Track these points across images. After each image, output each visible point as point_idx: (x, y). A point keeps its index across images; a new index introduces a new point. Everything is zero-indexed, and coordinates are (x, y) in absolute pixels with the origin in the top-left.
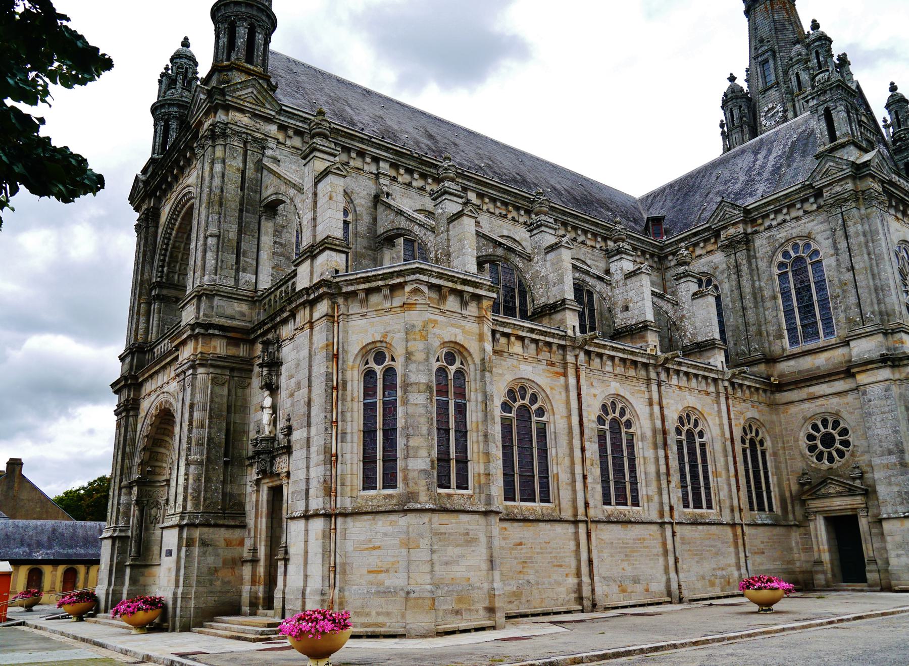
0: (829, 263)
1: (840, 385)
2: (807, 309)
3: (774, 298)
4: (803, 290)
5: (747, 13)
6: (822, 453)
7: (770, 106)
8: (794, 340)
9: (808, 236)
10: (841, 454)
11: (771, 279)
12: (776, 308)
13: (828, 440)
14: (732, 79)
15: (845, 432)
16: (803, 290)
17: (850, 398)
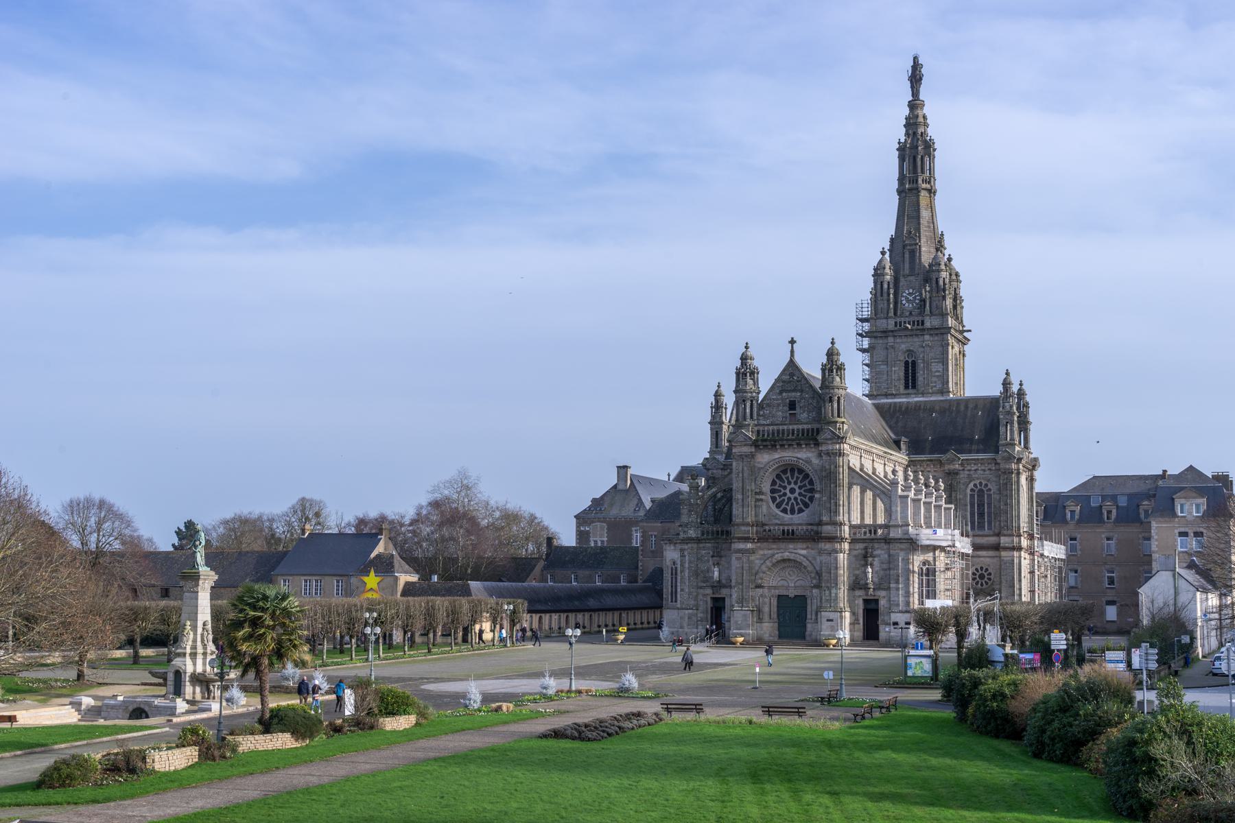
0: (995, 497)
1: (991, 553)
2: (981, 515)
3: (966, 505)
4: (981, 505)
5: (900, 192)
6: (978, 582)
7: (911, 291)
8: (973, 528)
9: (988, 480)
10: (987, 583)
11: (966, 494)
12: (966, 511)
13: (982, 577)
14: (883, 253)
15: (990, 574)
16: (981, 505)
17: (995, 560)
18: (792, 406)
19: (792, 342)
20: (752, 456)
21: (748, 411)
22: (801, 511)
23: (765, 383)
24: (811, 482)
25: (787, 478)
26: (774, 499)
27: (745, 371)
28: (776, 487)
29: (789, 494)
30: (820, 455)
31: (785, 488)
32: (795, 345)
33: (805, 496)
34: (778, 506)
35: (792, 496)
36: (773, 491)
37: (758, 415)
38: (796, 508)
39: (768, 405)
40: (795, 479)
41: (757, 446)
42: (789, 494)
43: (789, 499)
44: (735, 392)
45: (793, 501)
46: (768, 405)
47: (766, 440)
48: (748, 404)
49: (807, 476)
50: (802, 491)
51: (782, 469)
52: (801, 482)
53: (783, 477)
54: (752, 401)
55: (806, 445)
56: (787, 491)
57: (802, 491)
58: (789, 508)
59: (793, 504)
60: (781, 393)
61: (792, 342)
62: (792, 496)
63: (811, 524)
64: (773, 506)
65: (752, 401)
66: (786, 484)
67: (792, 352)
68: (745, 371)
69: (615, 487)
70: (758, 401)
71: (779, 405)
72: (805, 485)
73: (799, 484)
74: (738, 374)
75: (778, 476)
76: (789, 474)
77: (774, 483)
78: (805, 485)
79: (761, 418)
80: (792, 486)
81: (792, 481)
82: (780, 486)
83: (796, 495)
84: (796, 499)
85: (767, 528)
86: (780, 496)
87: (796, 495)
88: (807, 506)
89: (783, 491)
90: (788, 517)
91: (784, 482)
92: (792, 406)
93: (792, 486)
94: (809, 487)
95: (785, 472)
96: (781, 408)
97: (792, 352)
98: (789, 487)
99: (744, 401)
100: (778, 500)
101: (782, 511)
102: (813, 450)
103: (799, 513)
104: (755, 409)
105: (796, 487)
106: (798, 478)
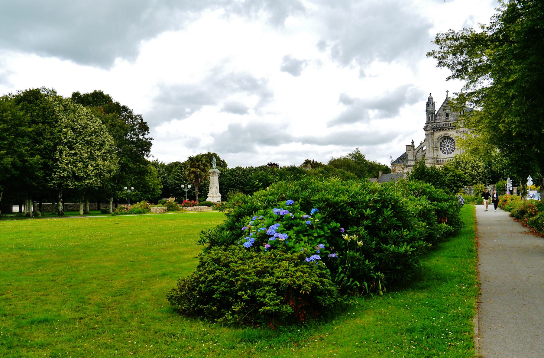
18: (447, 115)
19: (447, 92)
20: (433, 134)
21: (431, 118)
22: (451, 153)
23: (437, 107)
24: (454, 143)
25: (446, 141)
26: (441, 149)
27: (430, 103)
28: (442, 145)
29: (446, 147)
30: (457, 132)
31: (445, 145)
32: (448, 93)
33: (452, 148)
34: (443, 152)
35: (448, 148)
36: (441, 146)
37: (435, 119)
38: (449, 152)
39: (439, 115)
41: (434, 130)
42: (446, 147)
43: (446, 149)
44: (426, 111)
45: (448, 149)
46: (439, 115)
47: (437, 128)
48: (431, 115)
49: (453, 140)
53: (444, 141)
54: (432, 114)
55: (452, 129)
56: (446, 146)
58: (446, 152)
60: (443, 110)
61: (447, 92)
62: (448, 148)
64: (441, 152)
65: (432, 114)
67: (447, 95)
68: (430, 103)
69: (405, 153)
70: (434, 114)
71: (442, 115)
72: (452, 144)
73: (450, 143)
74: (427, 104)
75: (443, 141)
76: (446, 140)
77: (441, 143)
79: (436, 120)
80: (448, 144)
83: (449, 147)
84: (449, 149)
85: (438, 160)
87: (449, 147)
88: (453, 151)
90: (446, 156)
92: (447, 115)
93: (448, 144)
95: (445, 139)
96: (443, 116)
97: (447, 95)
98: (446, 145)
99: (429, 114)
100: (443, 150)
104: (433, 117)
105: (449, 144)
106: (449, 141)
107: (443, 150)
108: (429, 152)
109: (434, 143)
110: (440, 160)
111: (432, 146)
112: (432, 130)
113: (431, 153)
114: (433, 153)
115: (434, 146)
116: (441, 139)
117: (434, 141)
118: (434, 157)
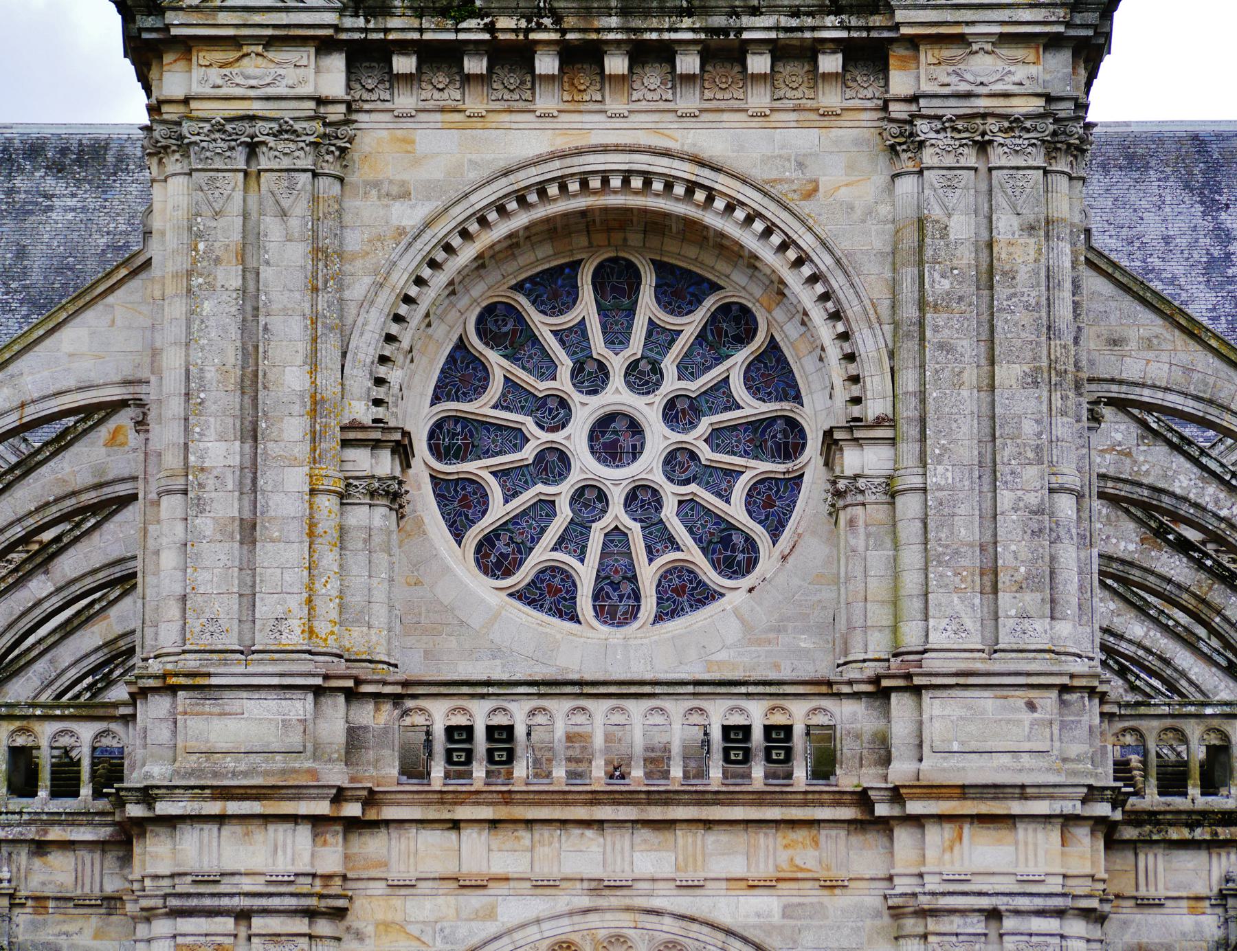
25: (574, 338)
28: (482, 407)
33: (722, 480)
38: (648, 574)
40: (636, 345)
45: (617, 513)
50: (696, 438)
51: (541, 259)
52: (686, 369)
53: (542, 324)
55: (780, 52)
57: (696, 438)
58: (586, 574)
59: (617, 535)
63: (826, 688)
66: (563, 383)
72: (720, 395)
73: (671, 384)
76: (586, 307)
78: (720, 395)
81: (617, 364)
82: (515, 395)
86: (512, 479)
89: (539, 438)
91: (547, 368)
94: (752, 407)
100: (498, 510)
101: (529, 596)
102: (831, 98)
103: (668, 610)
105: (648, 410)
107: (498, 510)
108: (249, 531)
109: (366, 345)
110: (480, 715)
111: (316, 405)
112: (325, 46)
113: (295, 552)
114: (329, 560)
115: (362, 412)
116: (452, 289)
117: (358, 289)
118: (356, 640)
